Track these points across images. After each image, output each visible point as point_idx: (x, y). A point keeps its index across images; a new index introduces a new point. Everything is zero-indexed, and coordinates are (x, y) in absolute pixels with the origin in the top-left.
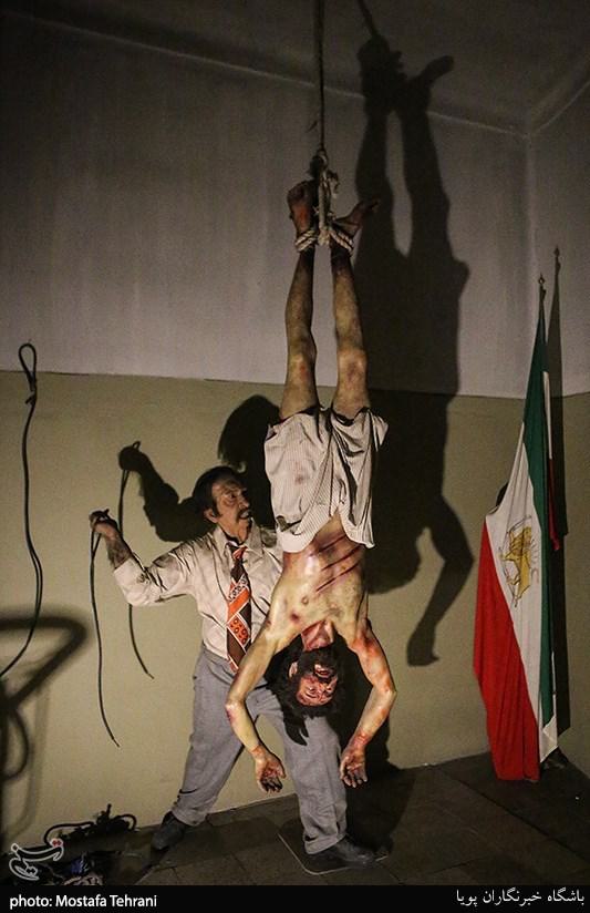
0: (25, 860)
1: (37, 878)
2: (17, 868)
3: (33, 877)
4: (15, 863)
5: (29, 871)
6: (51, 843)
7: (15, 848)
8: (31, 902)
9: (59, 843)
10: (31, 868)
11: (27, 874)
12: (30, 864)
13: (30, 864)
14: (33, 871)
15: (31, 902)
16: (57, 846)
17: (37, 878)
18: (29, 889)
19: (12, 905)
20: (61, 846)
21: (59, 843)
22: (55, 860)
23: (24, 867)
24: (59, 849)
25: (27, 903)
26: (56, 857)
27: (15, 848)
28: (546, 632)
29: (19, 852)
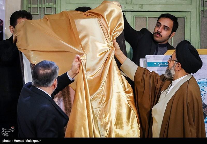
1: (8, 136)
2: (3, 133)
3: (7, 136)
4: (3, 132)
5: (6, 134)
6: (11, 128)
7: (3, 129)
8: (7, 141)
9: (13, 128)
10: (7, 134)
11: (5, 135)
15: (7, 141)
16: (13, 128)
17: (8, 136)
18: (6, 138)
19: (3, 142)
20: (14, 128)
21: (13, 128)
22: (12, 132)
23: (5, 133)
24: (13, 129)
25: (6, 141)
26: (13, 131)
27: (3, 129)
28: (110, 84)
29: (4, 130)
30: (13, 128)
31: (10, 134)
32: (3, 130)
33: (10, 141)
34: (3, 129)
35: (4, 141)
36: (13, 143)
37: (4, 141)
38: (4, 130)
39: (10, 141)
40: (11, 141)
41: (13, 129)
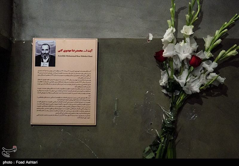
0: (6, 152)
1: (9, 157)
2: (4, 154)
3: (8, 156)
4: (3, 153)
5: (7, 155)
6: (13, 147)
7: (3, 148)
8: (8, 162)
9: (15, 147)
10: (8, 154)
12: (8, 153)
13: (8, 153)
14: (8, 155)
15: (8, 162)
16: (15, 148)
17: (9, 157)
18: (8, 160)
19: (3, 163)
20: (16, 148)
23: (6, 154)
24: (15, 149)
26: (15, 151)
27: (3, 148)
29: (5, 150)
30: (15, 147)
31: (11, 154)
32: (4, 150)
33: (11, 162)
34: (3, 148)
35: (4, 163)
36: (15, 164)
37: (4, 163)
38: (5, 150)
39: (11, 162)
40: (13, 163)
41: (15, 148)
